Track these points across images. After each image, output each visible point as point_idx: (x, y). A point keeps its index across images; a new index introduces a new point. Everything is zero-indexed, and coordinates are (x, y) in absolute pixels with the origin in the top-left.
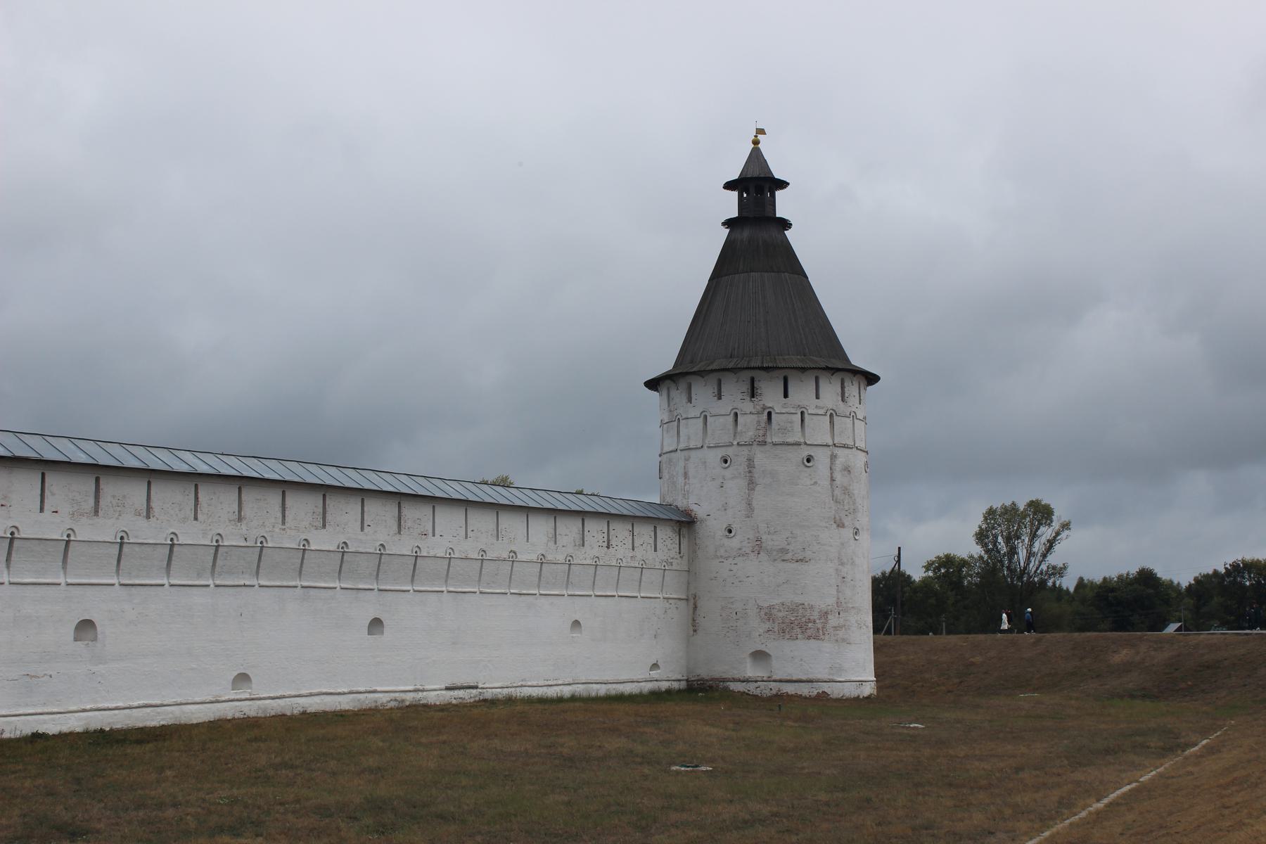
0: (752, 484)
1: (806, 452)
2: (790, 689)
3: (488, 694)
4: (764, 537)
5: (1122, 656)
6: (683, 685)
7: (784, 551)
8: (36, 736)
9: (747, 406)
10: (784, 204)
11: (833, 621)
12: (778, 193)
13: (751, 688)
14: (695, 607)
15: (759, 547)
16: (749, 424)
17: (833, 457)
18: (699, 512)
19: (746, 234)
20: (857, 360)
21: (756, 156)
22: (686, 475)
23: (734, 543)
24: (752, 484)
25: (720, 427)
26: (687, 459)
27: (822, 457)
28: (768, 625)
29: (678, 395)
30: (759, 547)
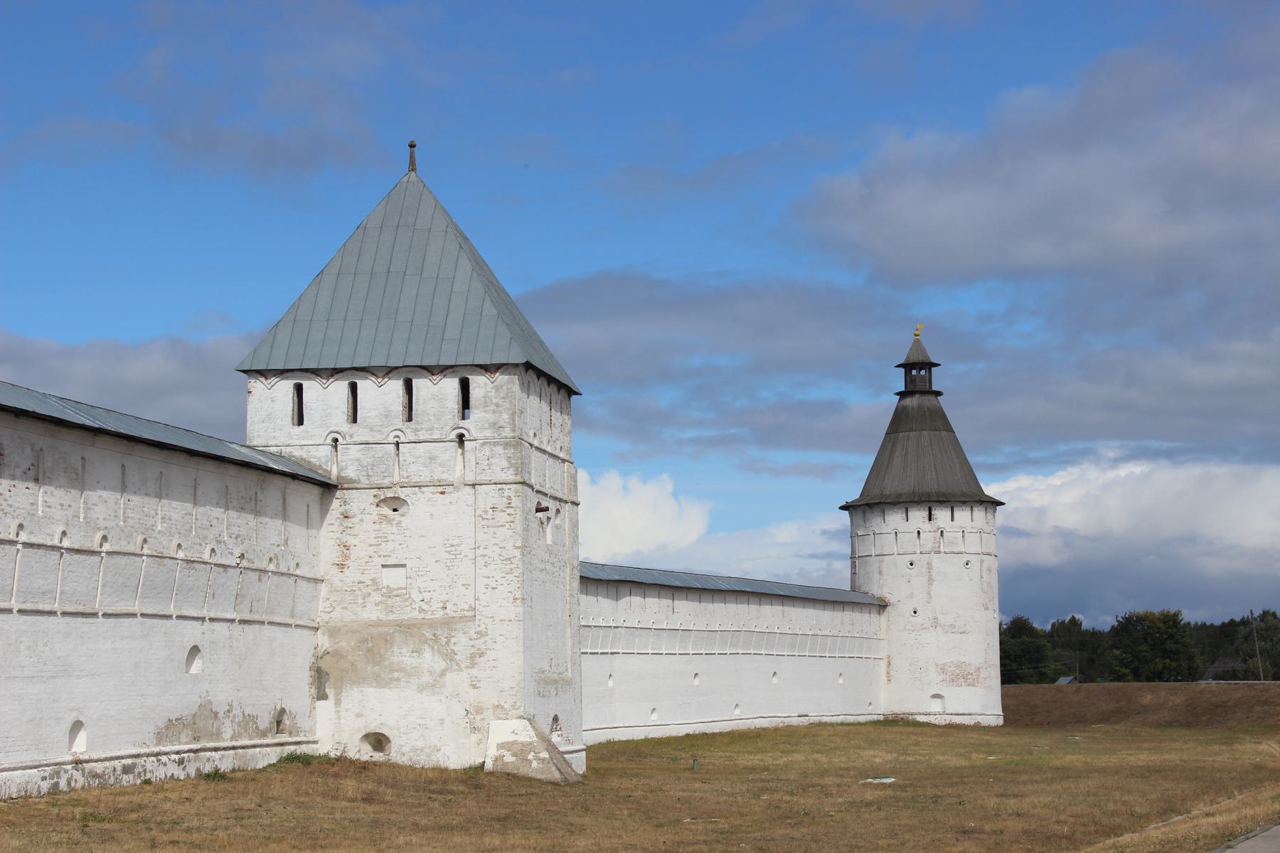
0: (931, 581)
1: (965, 558)
2: (957, 720)
3: (812, 720)
4: (940, 617)
5: (1148, 699)
6: (881, 718)
7: (952, 626)
8: (688, 735)
9: (926, 526)
10: (939, 380)
11: (983, 674)
12: (933, 369)
13: (931, 719)
14: (889, 664)
15: (936, 623)
16: (928, 538)
17: (982, 562)
18: (890, 598)
19: (911, 402)
20: (990, 490)
21: (917, 344)
22: (880, 573)
23: (919, 619)
24: (931, 581)
25: (908, 540)
26: (881, 562)
27: (975, 560)
28: (942, 676)
29: (859, 515)
30: (936, 623)
